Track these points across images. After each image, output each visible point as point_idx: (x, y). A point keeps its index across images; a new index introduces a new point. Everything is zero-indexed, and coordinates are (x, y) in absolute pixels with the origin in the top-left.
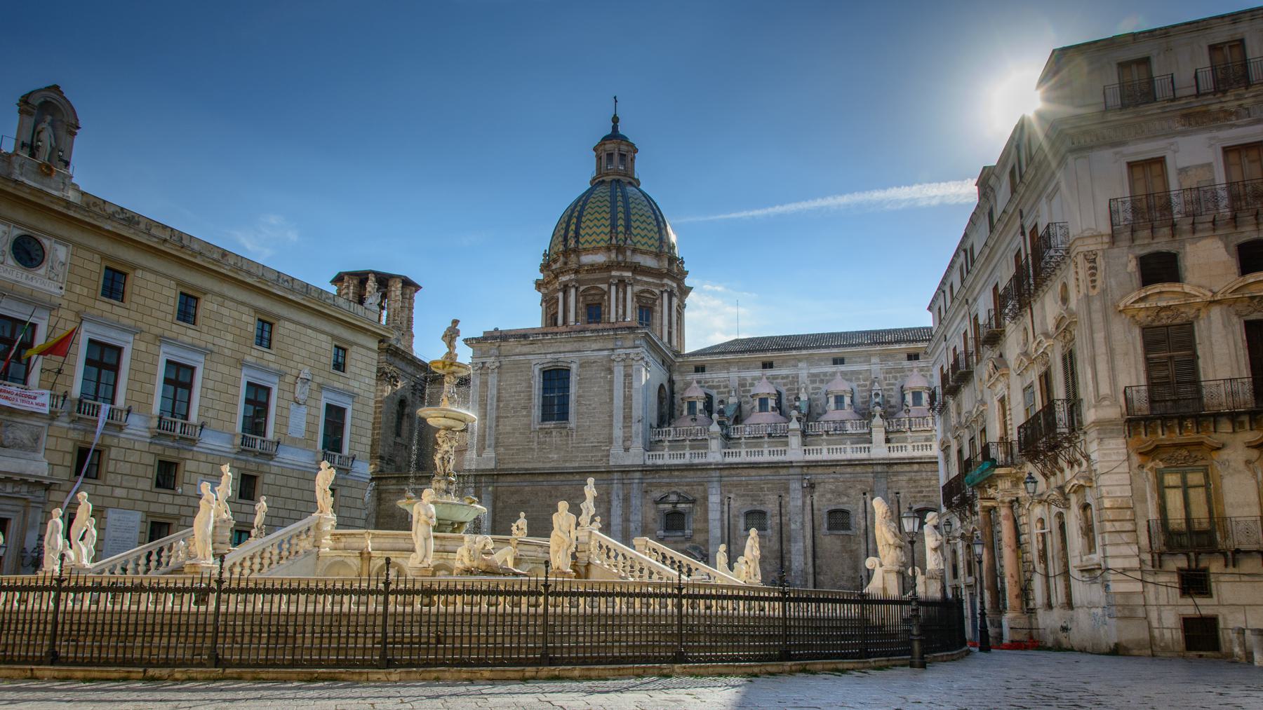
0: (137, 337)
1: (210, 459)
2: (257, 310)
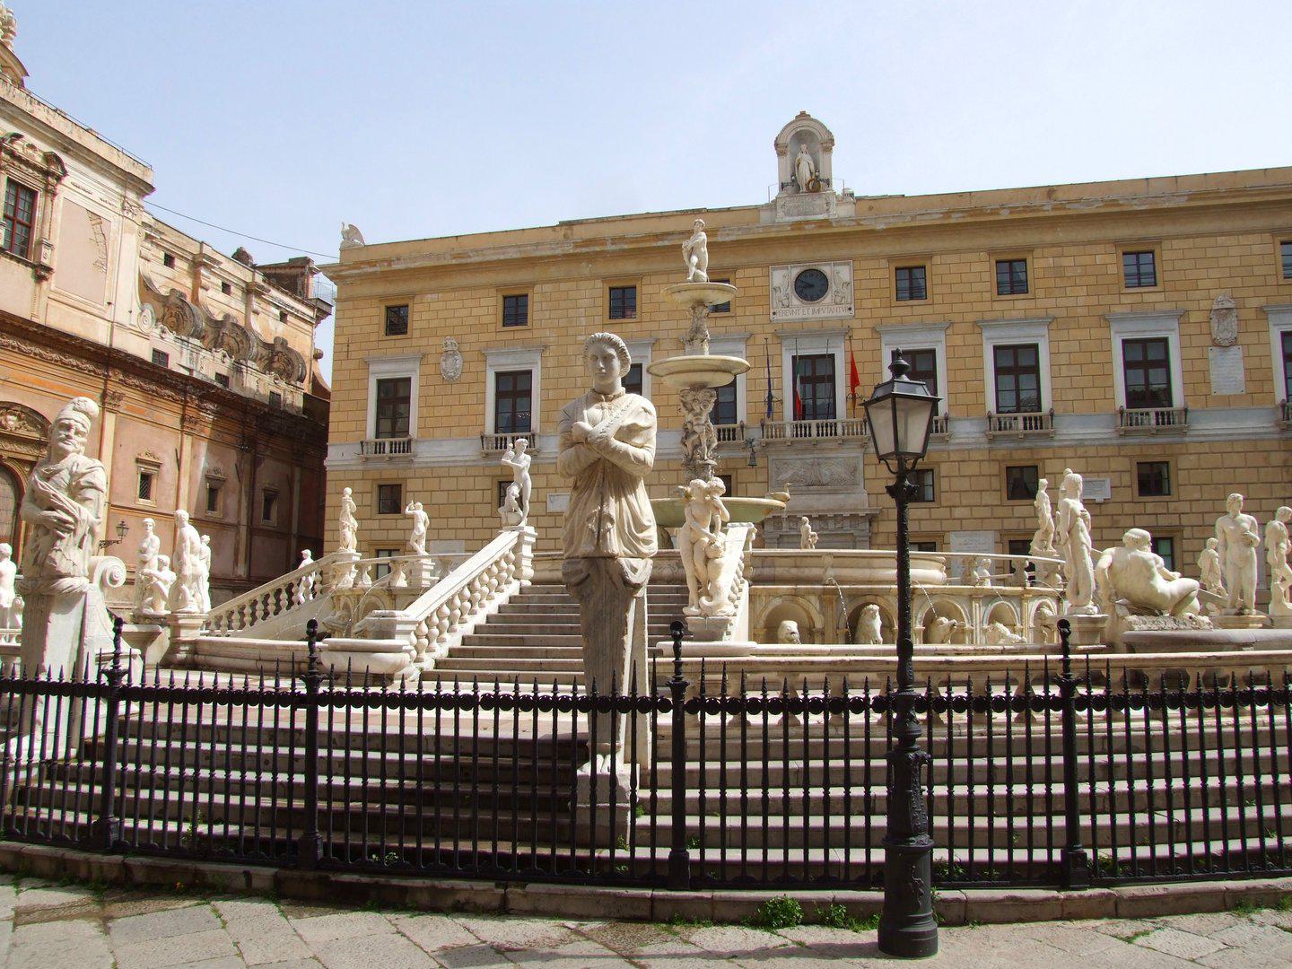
0: (949, 332)
1: (1080, 451)
2: (1116, 243)
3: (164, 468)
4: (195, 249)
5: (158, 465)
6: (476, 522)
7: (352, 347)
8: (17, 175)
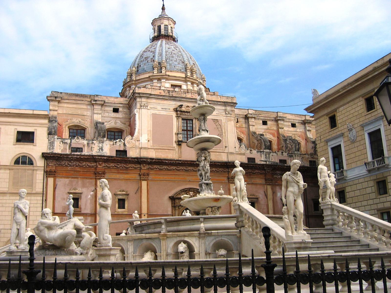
3: (260, 199)
4: (274, 115)
5: (257, 198)
6: (371, 202)
7: (322, 137)
8: (184, 117)
